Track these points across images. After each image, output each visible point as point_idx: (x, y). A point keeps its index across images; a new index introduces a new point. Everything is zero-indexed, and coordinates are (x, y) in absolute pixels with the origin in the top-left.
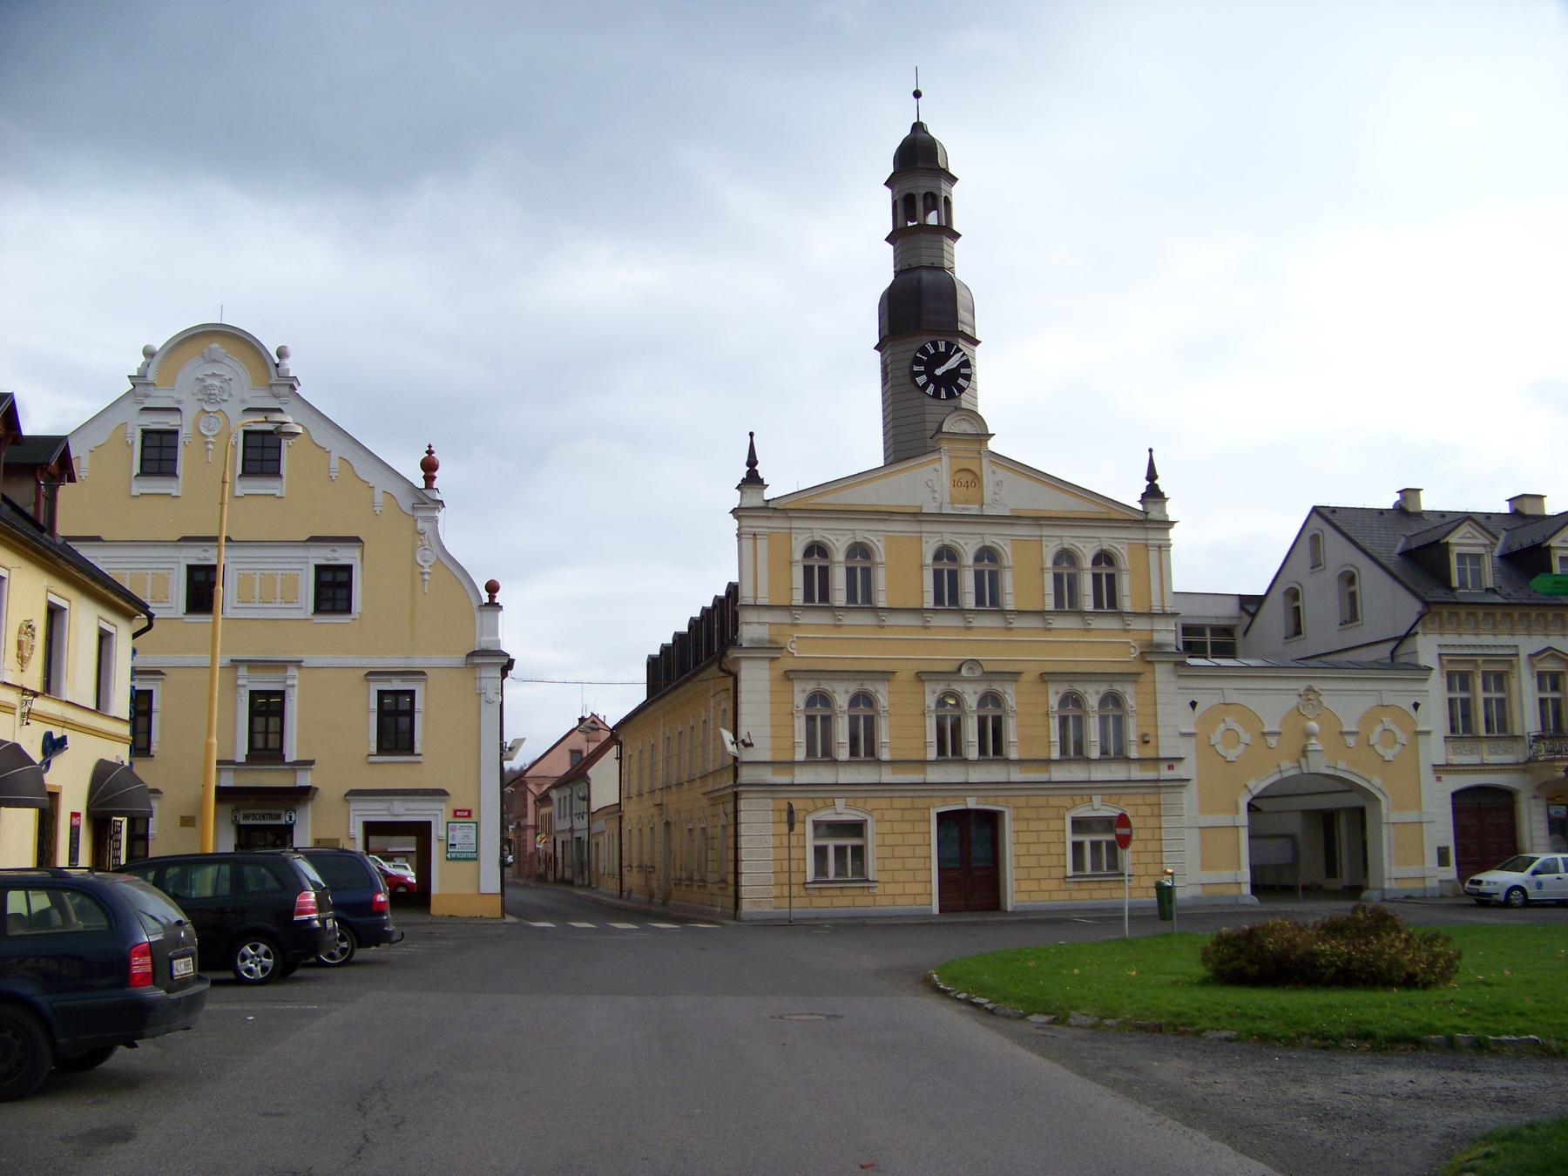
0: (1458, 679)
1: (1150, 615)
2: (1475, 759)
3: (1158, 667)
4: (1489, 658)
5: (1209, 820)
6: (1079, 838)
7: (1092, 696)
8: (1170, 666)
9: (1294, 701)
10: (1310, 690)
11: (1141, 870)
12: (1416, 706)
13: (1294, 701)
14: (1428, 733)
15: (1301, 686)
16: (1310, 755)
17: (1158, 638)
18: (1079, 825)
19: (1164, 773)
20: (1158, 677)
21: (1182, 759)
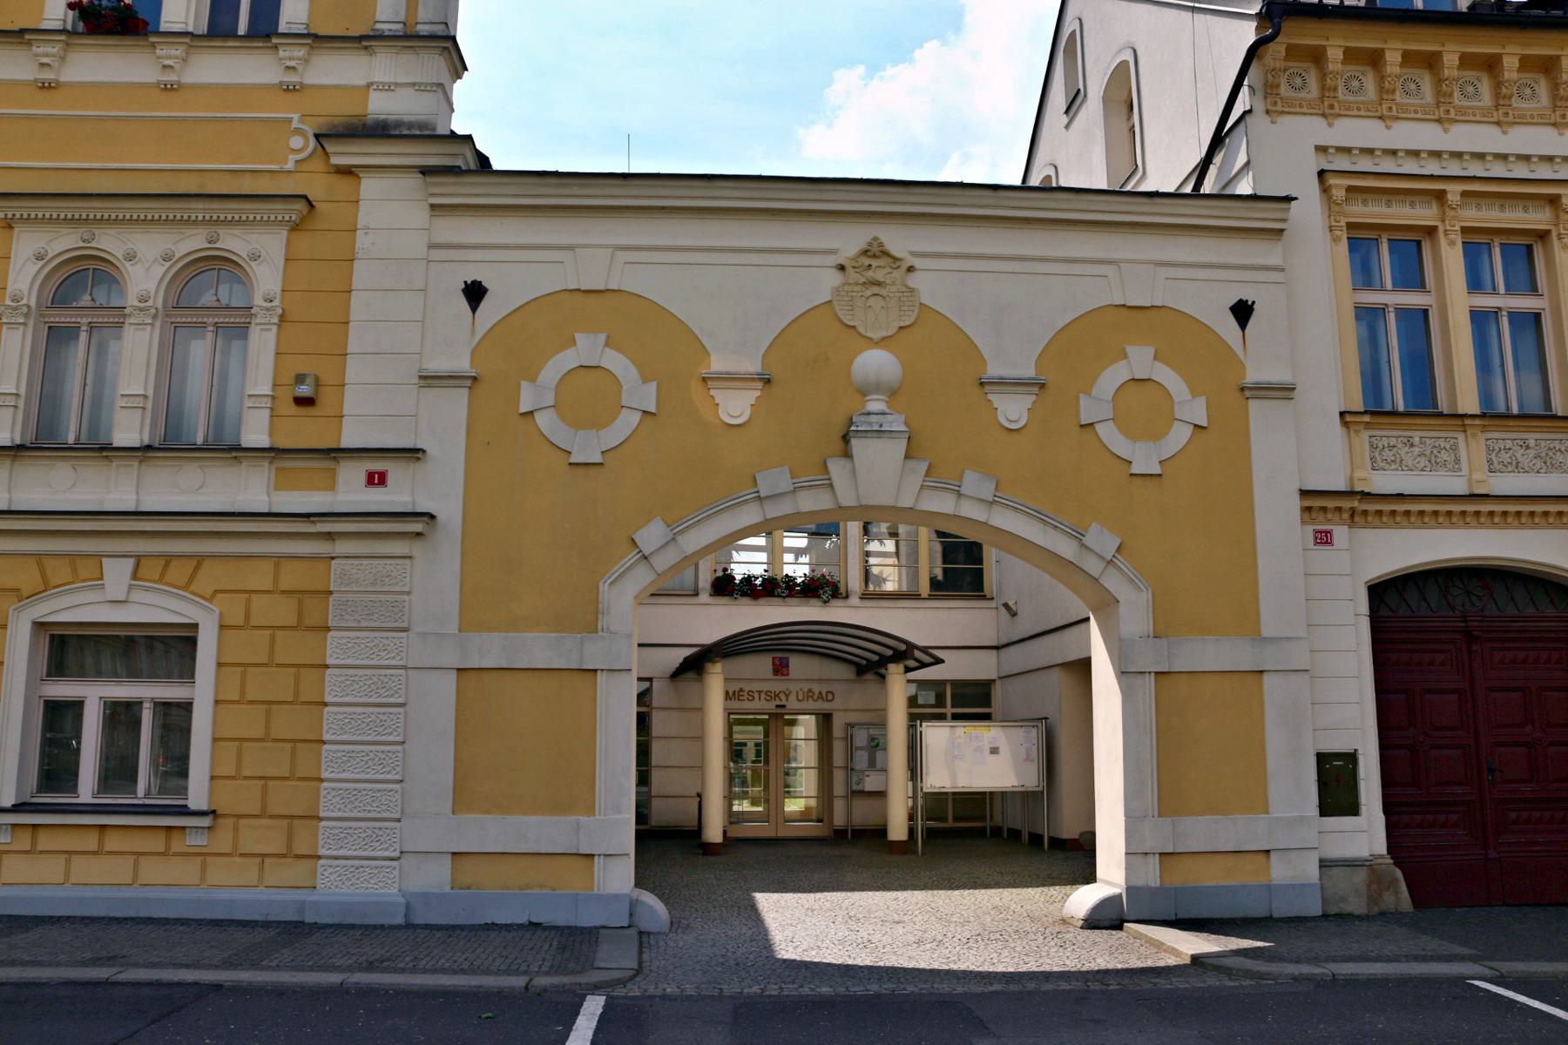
0: (1385, 248)
1: (367, 41)
2: (1458, 486)
3: (370, 186)
4: (1483, 192)
5: (490, 650)
6: (63, 690)
7: (145, 261)
8: (413, 182)
10: (875, 252)
11: (243, 798)
12: (1243, 312)
14: (1285, 391)
15: (849, 240)
17: (380, 106)
18: (66, 649)
19: (349, 490)
20: (367, 214)
21: (414, 454)
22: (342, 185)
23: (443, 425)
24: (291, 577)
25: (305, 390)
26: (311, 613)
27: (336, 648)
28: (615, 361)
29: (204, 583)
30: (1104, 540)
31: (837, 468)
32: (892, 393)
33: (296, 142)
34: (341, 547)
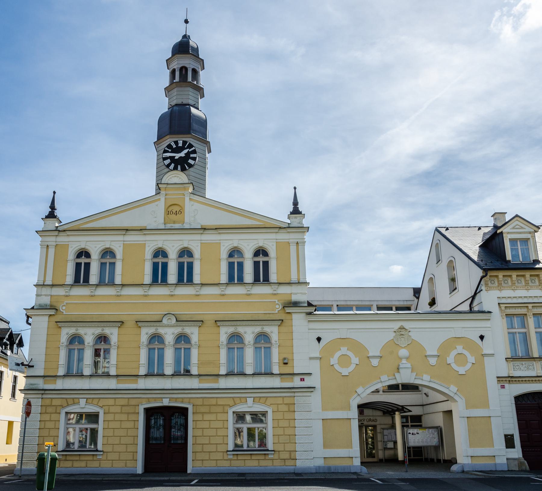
1: (290, 284)
8: (304, 315)
9: (392, 335)
13: (392, 335)
16: (401, 370)
17: (294, 298)
19: (296, 382)
22: (288, 316)
23: (315, 368)
24: (287, 401)
25: (286, 361)
26: (291, 408)
27: (297, 415)
28: (350, 354)
29: (269, 401)
30: (454, 388)
31: (397, 375)
32: (407, 358)
33: (277, 306)
34: (296, 394)
